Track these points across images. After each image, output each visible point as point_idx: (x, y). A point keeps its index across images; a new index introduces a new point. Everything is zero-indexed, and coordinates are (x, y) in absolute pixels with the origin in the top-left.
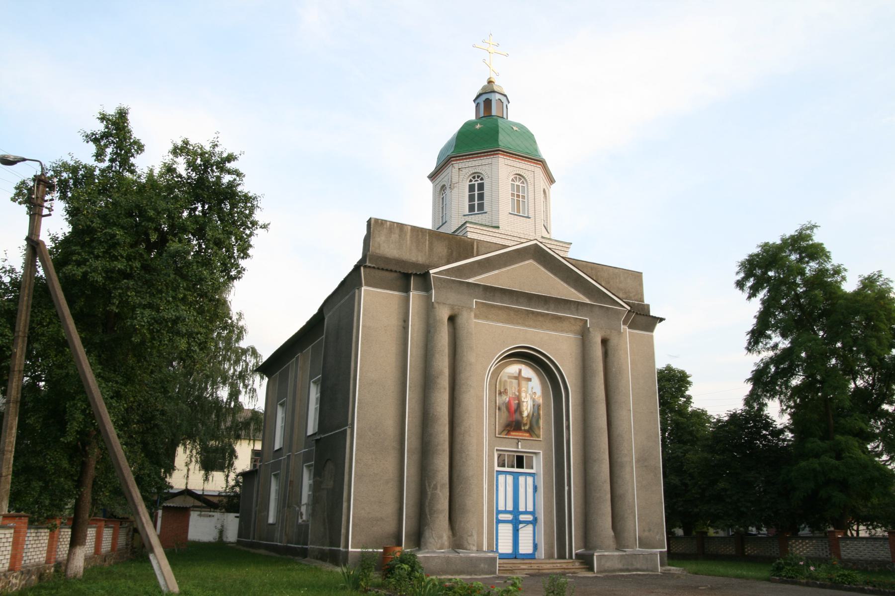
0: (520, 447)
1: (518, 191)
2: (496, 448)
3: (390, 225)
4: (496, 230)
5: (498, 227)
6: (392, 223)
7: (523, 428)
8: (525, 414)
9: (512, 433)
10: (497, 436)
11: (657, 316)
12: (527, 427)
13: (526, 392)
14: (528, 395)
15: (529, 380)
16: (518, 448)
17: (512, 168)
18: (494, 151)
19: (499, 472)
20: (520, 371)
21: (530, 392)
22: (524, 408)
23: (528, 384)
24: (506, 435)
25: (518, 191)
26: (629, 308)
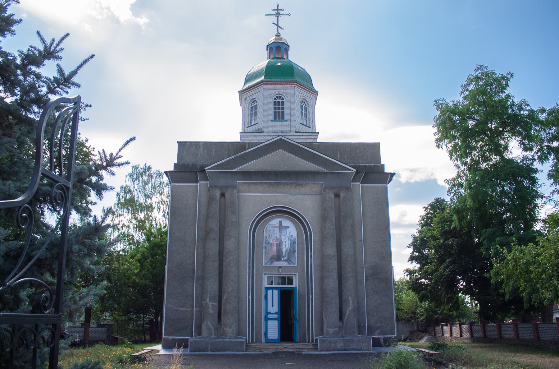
0: (280, 272)
1: (279, 105)
2: (263, 273)
3: (190, 144)
4: (261, 134)
5: (263, 132)
6: (191, 143)
7: (282, 259)
8: (284, 250)
9: (274, 263)
10: (264, 265)
11: (389, 172)
12: (285, 258)
13: (285, 235)
14: (286, 237)
15: (288, 227)
16: (279, 272)
17: (273, 91)
19: (267, 289)
20: (280, 222)
21: (288, 235)
22: (284, 246)
23: (286, 230)
24: (270, 264)
25: (279, 105)
26: (355, 170)
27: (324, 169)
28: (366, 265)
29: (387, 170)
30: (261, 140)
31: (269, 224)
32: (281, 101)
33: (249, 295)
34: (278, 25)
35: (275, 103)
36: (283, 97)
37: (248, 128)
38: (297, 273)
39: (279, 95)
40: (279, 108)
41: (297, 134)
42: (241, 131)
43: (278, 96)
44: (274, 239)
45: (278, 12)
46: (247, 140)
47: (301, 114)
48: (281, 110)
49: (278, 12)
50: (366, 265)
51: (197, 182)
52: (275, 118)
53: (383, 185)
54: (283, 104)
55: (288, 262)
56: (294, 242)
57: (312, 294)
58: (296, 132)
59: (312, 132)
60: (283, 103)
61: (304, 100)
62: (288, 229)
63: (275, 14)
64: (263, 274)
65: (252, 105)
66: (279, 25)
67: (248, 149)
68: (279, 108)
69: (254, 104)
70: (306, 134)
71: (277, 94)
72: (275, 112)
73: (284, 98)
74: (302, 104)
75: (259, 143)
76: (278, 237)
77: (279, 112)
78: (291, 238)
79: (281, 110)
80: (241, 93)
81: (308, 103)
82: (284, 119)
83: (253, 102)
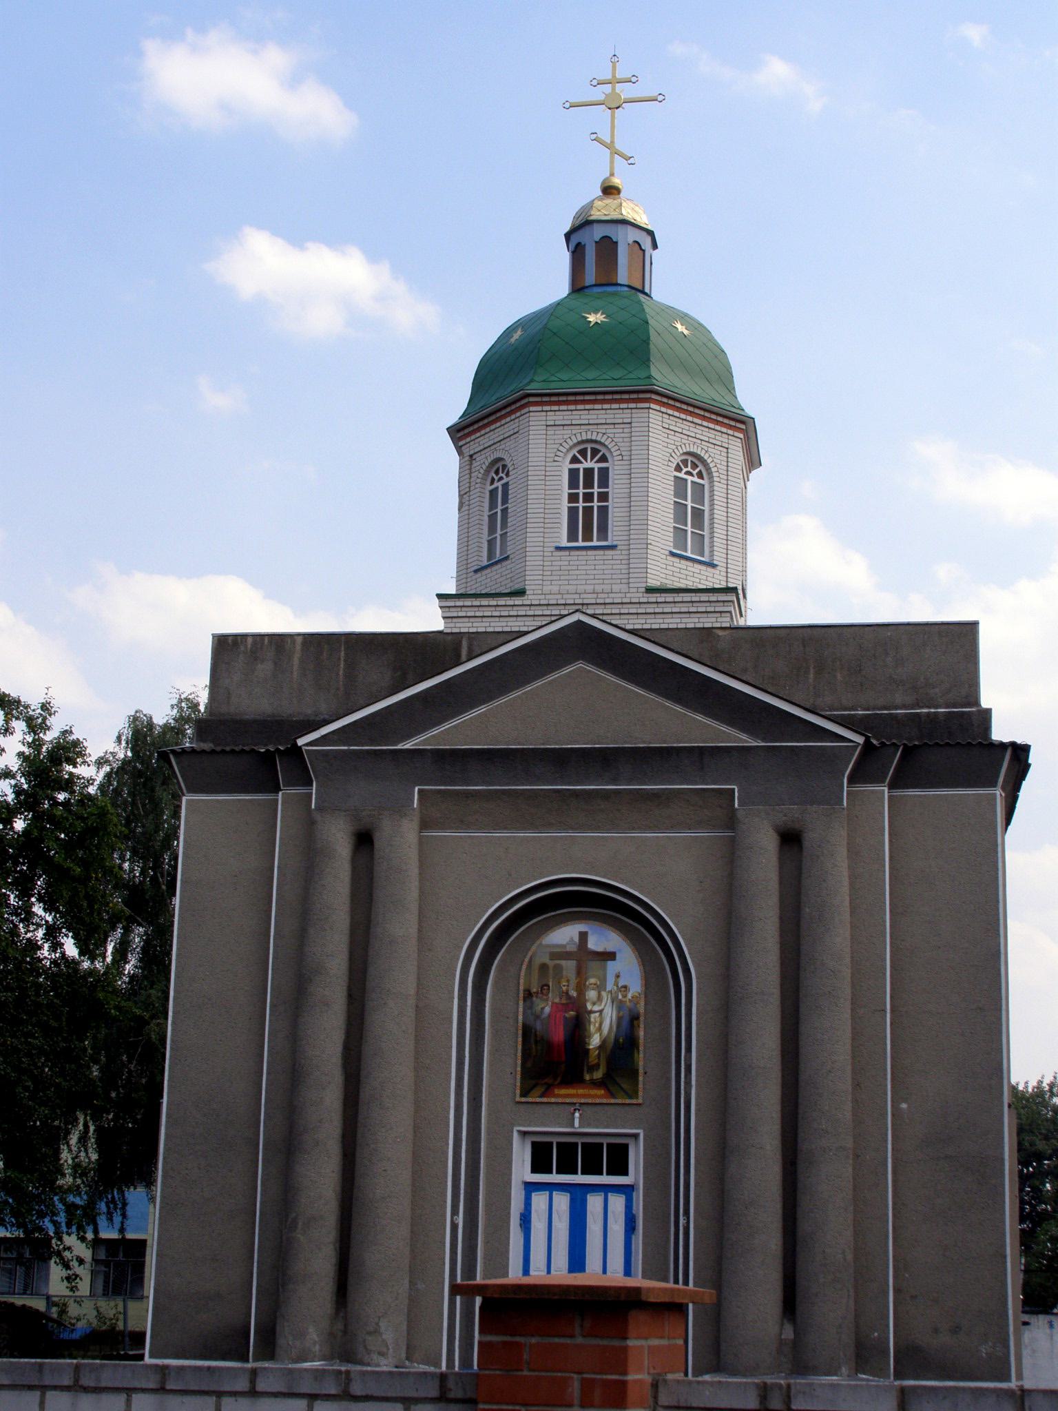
0: (577, 1123)
1: (589, 483)
2: (516, 1129)
3: (255, 643)
4: (518, 601)
5: (521, 593)
6: (258, 638)
7: (587, 1077)
8: (595, 1041)
9: (556, 1091)
10: (518, 1099)
11: (1006, 740)
12: (598, 1075)
13: (600, 988)
14: (604, 994)
15: (611, 956)
16: (573, 1126)
17: (567, 432)
18: (505, 407)
19: (530, 1187)
20: (583, 936)
21: (610, 985)
22: (592, 1029)
23: (604, 969)
24: (542, 1096)
25: (589, 483)
26: (860, 740)
27: (744, 736)
28: (904, 1106)
29: (1000, 733)
30: (515, 625)
31: (541, 944)
32: (596, 466)
33: (455, 1211)
34: (610, 146)
35: (573, 474)
36: (603, 450)
37: (479, 575)
38: (641, 1132)
39: (589, 446)
40: (588, 497)
41: (653, 598)
42: (452, 590)
43: (574, 455)
44: (557, 1000)
45: (614, 89)
46: (464, 627)
47: (675, 514)
48: (596, 504)
49: (614, 89)
50: (904, 1106)
51: (277, 789)
52: (572, 536)
53: (981, 791)
54: (604, 482)
55: (609, 1090)
56: (634, 1018)
57: (687, 1213)
58: (650, 590)
59: (723, 585)
60: (604, 473)
61: (690, 459)
62: (610, 963)
63: (602, 97)
64: (515, 1134)
65: (493, 481)
66: (618, 146)
67: (470, 659)
68: (588, 497)
69: (501, 479)
70: (687, 597)
71: (583, 442)
72: (573, 512)
73: (608, 455)
74: (682, 475)
75: (502, 638)
76: (574, 994)
77: (588, 511)
78: (620, 997)
79: (596, 504)
80: (459, 433)
81: (708, 469)
82: (606, 539)
83: (497, 472)
